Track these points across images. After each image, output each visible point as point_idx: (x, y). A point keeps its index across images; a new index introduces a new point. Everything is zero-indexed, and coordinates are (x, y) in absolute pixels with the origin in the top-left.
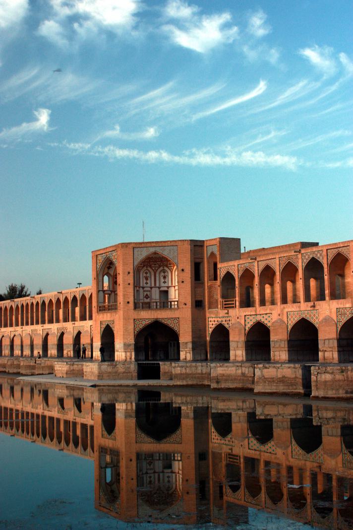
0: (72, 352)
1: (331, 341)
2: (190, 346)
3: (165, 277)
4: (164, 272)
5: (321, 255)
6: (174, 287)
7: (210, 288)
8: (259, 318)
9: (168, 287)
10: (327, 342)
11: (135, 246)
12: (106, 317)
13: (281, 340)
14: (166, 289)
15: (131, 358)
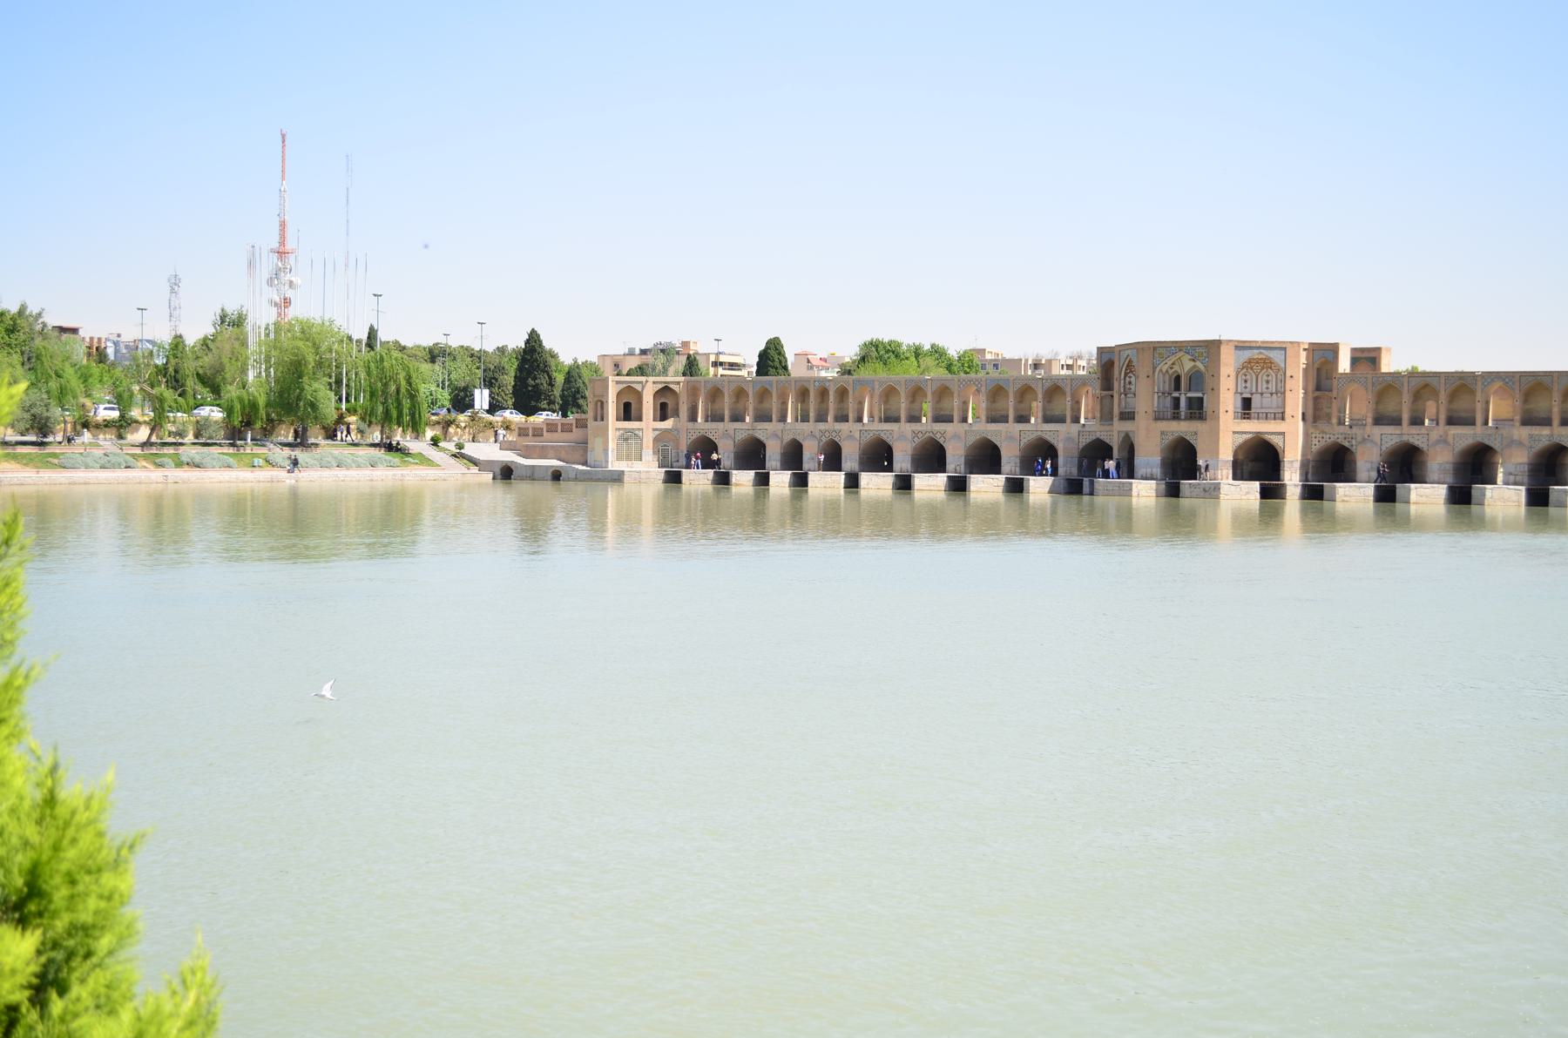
0: (963, 467)
1: (1522, 466)
2: (1297, 465)
3: (1246, 381)
4: (1246, 375)
5: (1510, 380)
6: (1262, 394)
7: (1316, 399)
8: (1405, 438)
9: (1252, 394)
10: (1518, 467)
11: (1236, 343)
12: (1182, 428)
13: (1447, 463)
14: (1248, 396)
15: (1227, 478)
